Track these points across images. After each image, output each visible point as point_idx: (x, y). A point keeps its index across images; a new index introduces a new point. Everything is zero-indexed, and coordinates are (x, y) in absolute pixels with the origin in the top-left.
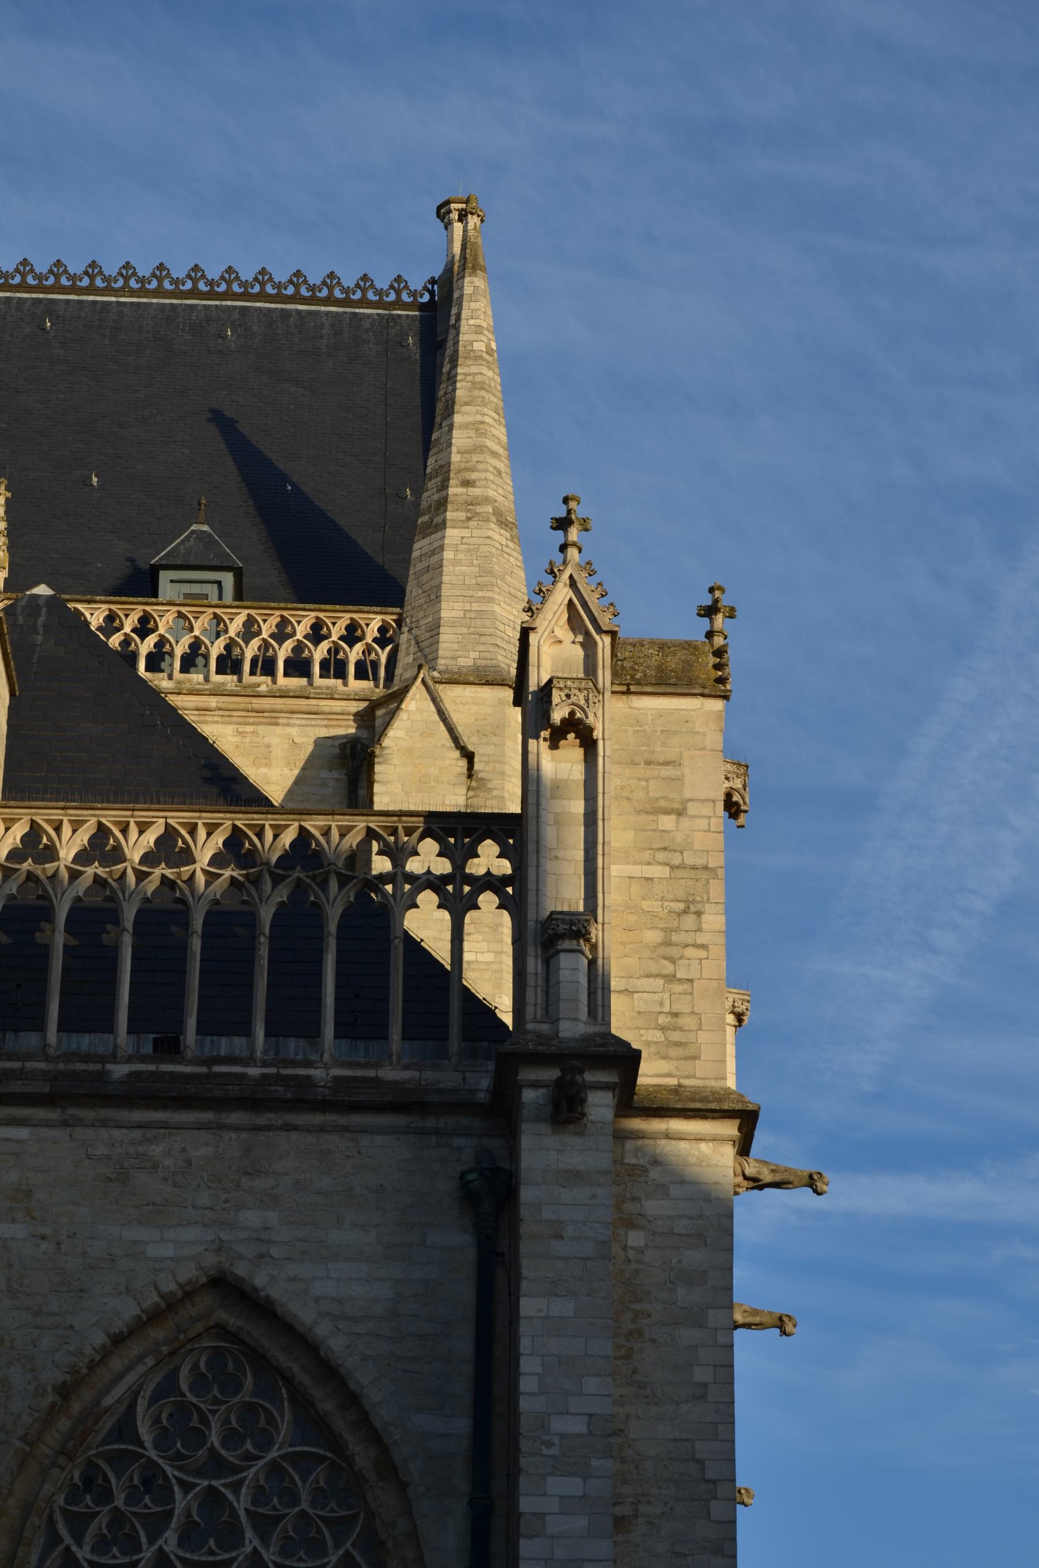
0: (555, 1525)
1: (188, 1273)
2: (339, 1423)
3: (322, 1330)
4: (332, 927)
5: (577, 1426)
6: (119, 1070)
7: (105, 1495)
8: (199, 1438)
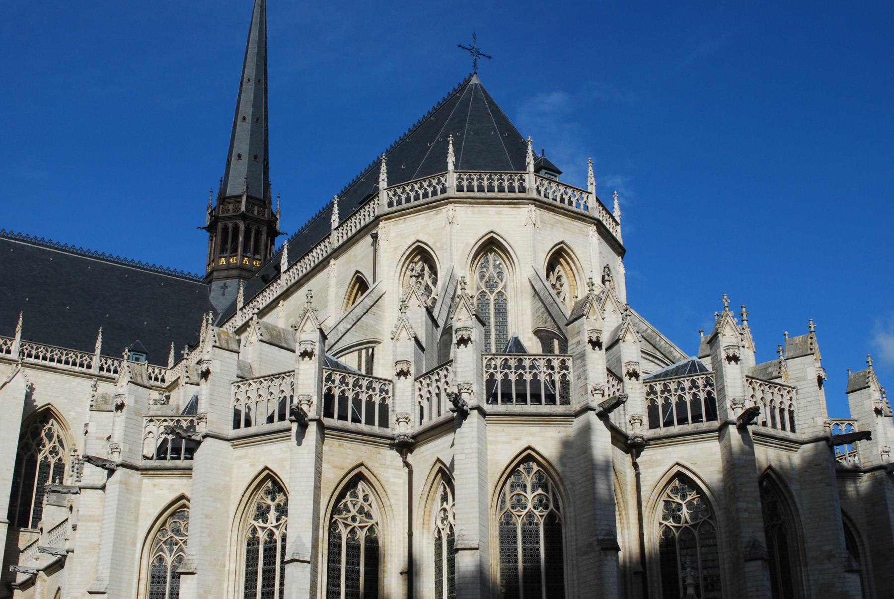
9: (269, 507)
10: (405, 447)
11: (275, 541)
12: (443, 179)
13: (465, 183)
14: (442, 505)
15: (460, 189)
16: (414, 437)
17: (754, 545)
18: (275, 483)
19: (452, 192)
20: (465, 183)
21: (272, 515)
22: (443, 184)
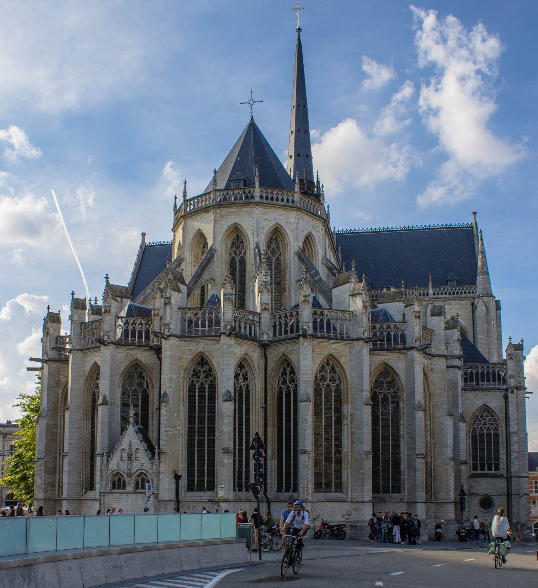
0: (513, 425)
1: (482, 404)
2: (494, 415)
3: (493, 408)
4: (491, 374)
5: (514, 418)
6: (475, 387)
7: (476, 422)
8: (483, 417)
9: (200, 371)
10: (264, 346)
11: (205, 388)
12: (252, 191)
13: (264, 195)
14: (282, 375)
15: (261, 197)
16: (271, 342)
17: (419, 402)
18: (203, 359)
19: (257, 199)
20: (264, 195)
21: (202, 375)
22: (252, 194)
